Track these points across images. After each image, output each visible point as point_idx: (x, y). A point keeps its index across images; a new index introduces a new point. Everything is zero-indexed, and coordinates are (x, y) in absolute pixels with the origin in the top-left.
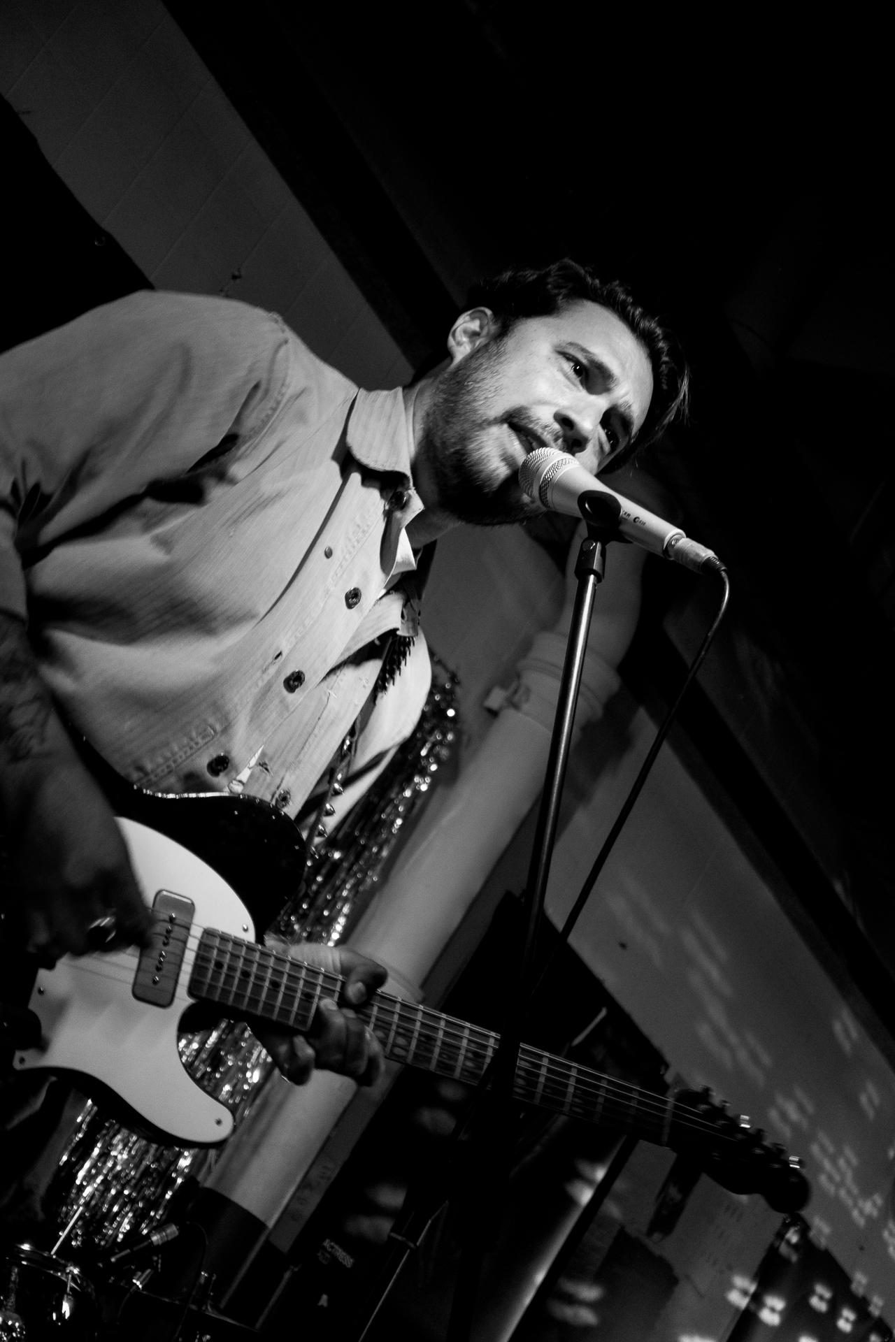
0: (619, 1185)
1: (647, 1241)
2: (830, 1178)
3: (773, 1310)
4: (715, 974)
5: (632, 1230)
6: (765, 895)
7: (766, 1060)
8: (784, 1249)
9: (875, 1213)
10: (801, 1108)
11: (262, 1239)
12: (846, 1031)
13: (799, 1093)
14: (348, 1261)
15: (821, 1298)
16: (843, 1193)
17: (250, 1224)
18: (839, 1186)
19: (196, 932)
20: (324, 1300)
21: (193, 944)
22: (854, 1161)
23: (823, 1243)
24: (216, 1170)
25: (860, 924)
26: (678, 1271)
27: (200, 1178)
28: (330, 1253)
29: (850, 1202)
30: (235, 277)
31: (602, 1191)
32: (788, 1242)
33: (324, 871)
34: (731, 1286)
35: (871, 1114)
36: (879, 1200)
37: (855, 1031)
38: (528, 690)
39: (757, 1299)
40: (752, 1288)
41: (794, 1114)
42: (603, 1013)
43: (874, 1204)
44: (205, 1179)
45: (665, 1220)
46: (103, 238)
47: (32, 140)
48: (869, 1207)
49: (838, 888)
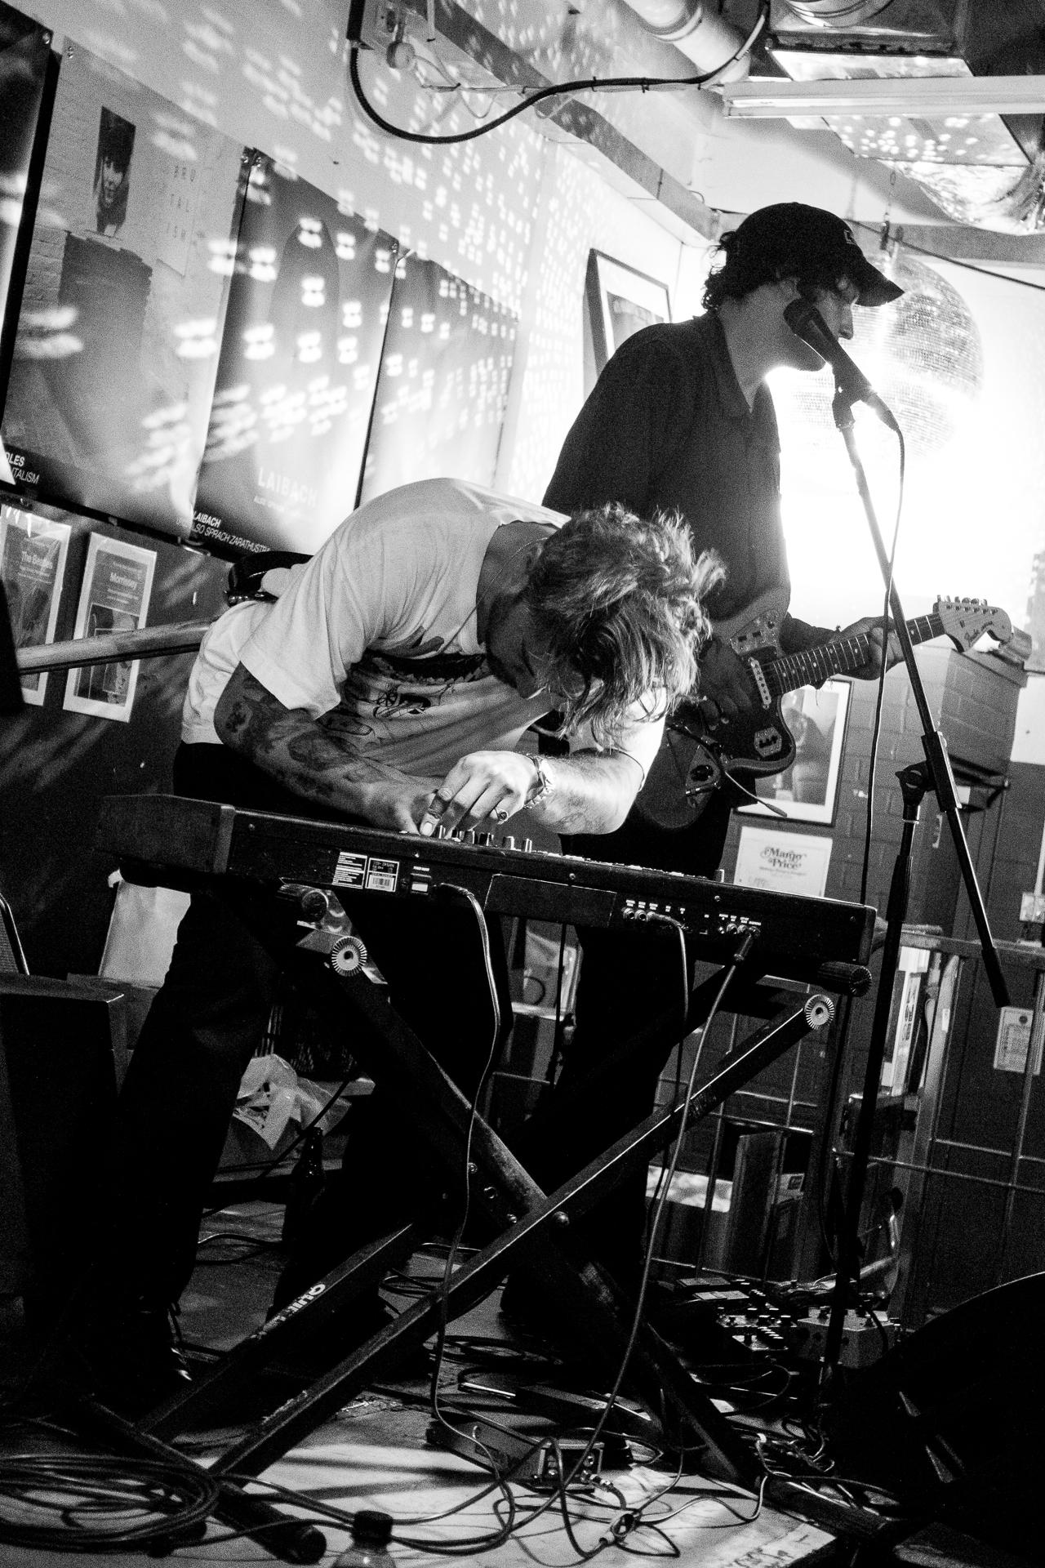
0: (47, 189)
1: (99, 239)
2: (277, 99)
3: (264, 264)
8: (253, 194)
9: (338, 120)
10: (219, 32)
13: (209, 14)
16: (295, 110)
18: (288, 103)
22: (297, 70)
26: (147, 260)
29: (305, 117)
32: (255, 186)
34: (210, 255)
39: (241, 257)
41: (213, 41)
43: (334, 110)
45: (112, 210)
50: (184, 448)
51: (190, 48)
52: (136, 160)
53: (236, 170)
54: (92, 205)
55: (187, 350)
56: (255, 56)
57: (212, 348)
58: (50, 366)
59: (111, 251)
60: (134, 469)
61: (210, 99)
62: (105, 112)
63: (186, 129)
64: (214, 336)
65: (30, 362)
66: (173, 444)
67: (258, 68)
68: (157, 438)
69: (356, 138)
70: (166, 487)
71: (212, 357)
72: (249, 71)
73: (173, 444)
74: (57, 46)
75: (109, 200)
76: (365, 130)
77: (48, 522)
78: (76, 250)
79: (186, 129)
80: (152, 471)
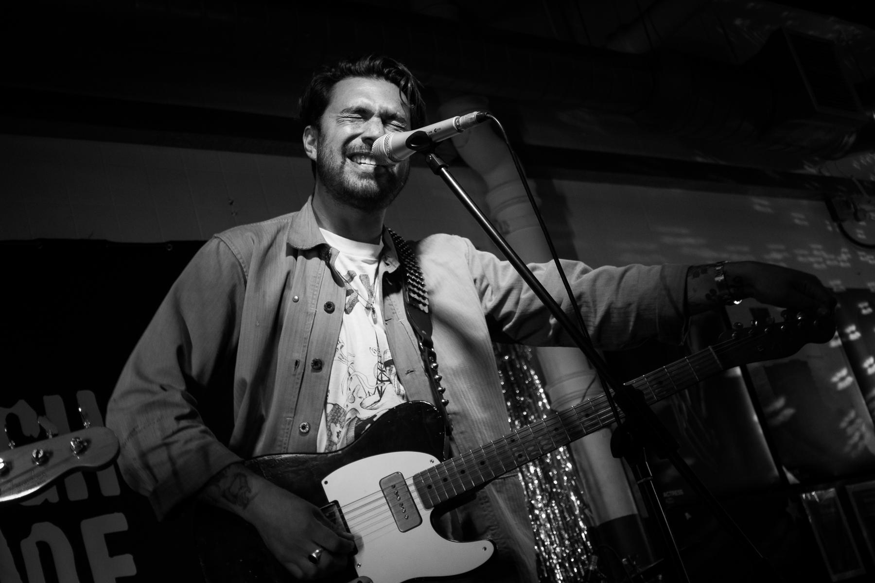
2: (819, 263)
3: (853, 332)
4: (690, 241)
6: (676, 193)
7: (746, 249)
9: (849, 256)
10: (779, 251)
11: (640, 523)
12: (761, 205)
14: (680, 492)
15: (865, 308)
16: (829, 263)
17: (628, 521)
20: (688, 516)
22: (819, 247)
23: (843, 288)
24: (595, 515)
25: (722, 163)
27: (593, 525)
29: (835, 263)
30: (231, 204)
33: (509, 368)
35: (806, 223)
36: (844, 250)
37: (765, 202)
38: (505, 222)
43: (845, 253)
44: (595, 523)
46: (169, 245)
47: (104, 242)
48: (844, 257)
49: (699, 159)
50: (864, 428)
55: (841, 386)
56: (801, 252)
57: (850, 380)
60: (847, 449)
64: (849, 374)
67: (803, 256)
68: (850, 430)
69: (862, 259)
70: (866, 449)
72: (801, 259)
73: (858, 429)
76: (863, 253)
77: (823, 492)
80: (855, 446)
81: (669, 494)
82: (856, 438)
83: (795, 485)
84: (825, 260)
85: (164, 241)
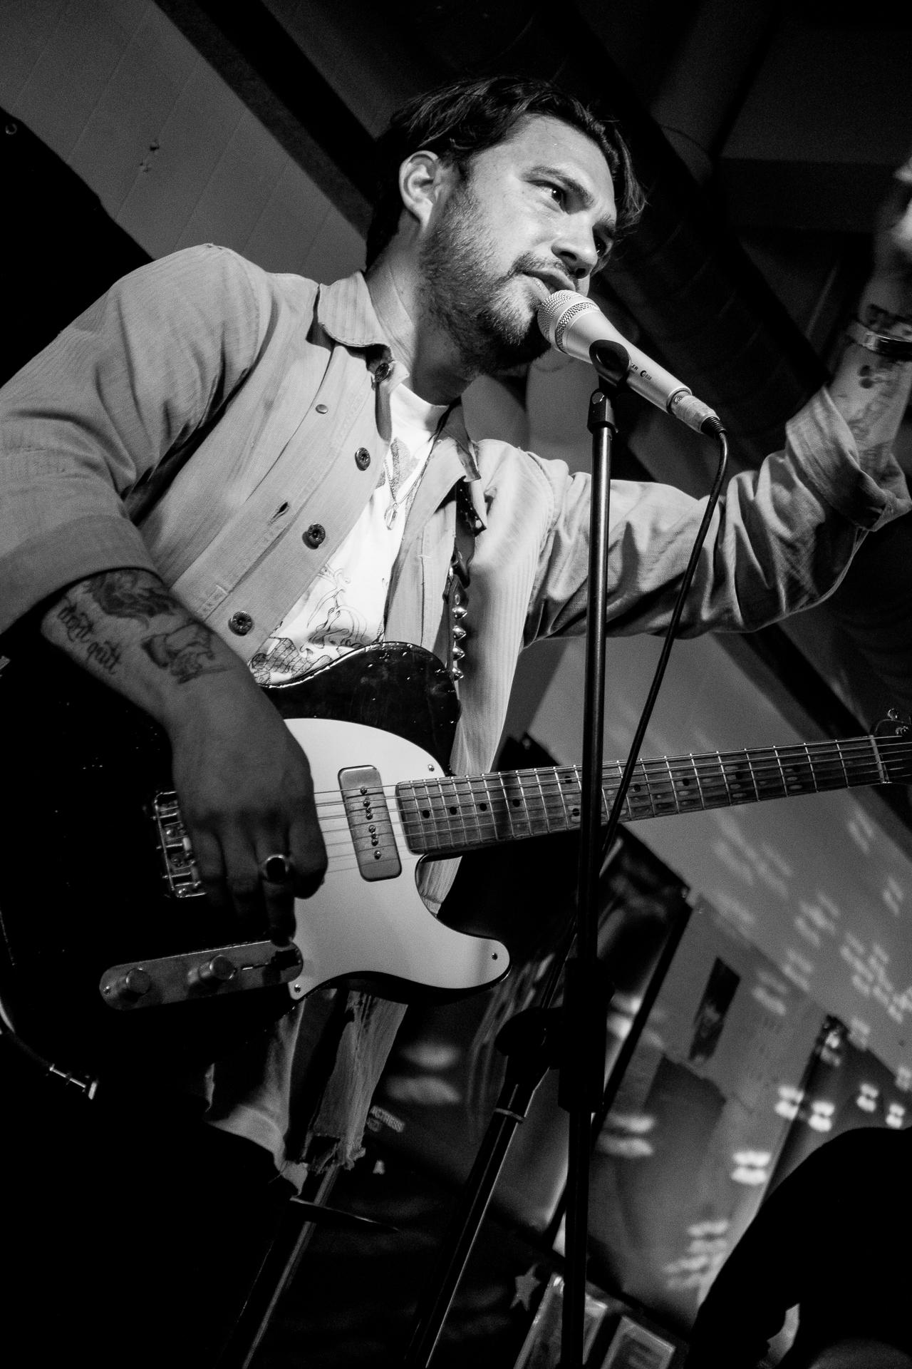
0: (656, 1014)
1: (690, 1066)
2: (864, 979)
3: (822, 1116)
5: (675, 1057)
7: (786, 870)
8: (825, 1055)
10: (827, 914)
13: (823, 899)
14: (397, 1125)
15: (868, 1097)
19: (390, 791)
21: (392, 804)
22: (885, 959)
26: (725, 1090)
28: (379, 1120)
29: (885, 1000)
30: (153, 149)
31: (640, 1022)
32: (830, 1048)
34: (778, 1098)
35: (895, 909)
37: (870, 829)
39: (805, 1107)
40: (799, 1097)
41: (819, 919)
42: (619, 844)
45: (705, 1043)
46: (14, 126)
49: (837, 689)
51: (800, 923)
52: (734, 1007)
53: (815, 1031)
54: (687, 1037)
55: (741, 1175)
56: (855, 942)
58: (622, 1162)
59: (696, 1078)
60: (671, 1268)
61: (808, 967)
62: (719, 963)
63: (782, 988)
64: (766, 1168)
65: (605, 1156)
66: (709, 1255)
67: (853, 950)
68: (697, 1246)
71: (760, 1186)
72: (845, 952)
74: (691, 899)
75: (704, 1035)
78: (668, 1071)
79: (782, 988)
80: (686, 1274)
81: (381, 1114)
82: (696, 1264)
83: (557, 1254)
84: (875, 983)
85: (11, 112)
